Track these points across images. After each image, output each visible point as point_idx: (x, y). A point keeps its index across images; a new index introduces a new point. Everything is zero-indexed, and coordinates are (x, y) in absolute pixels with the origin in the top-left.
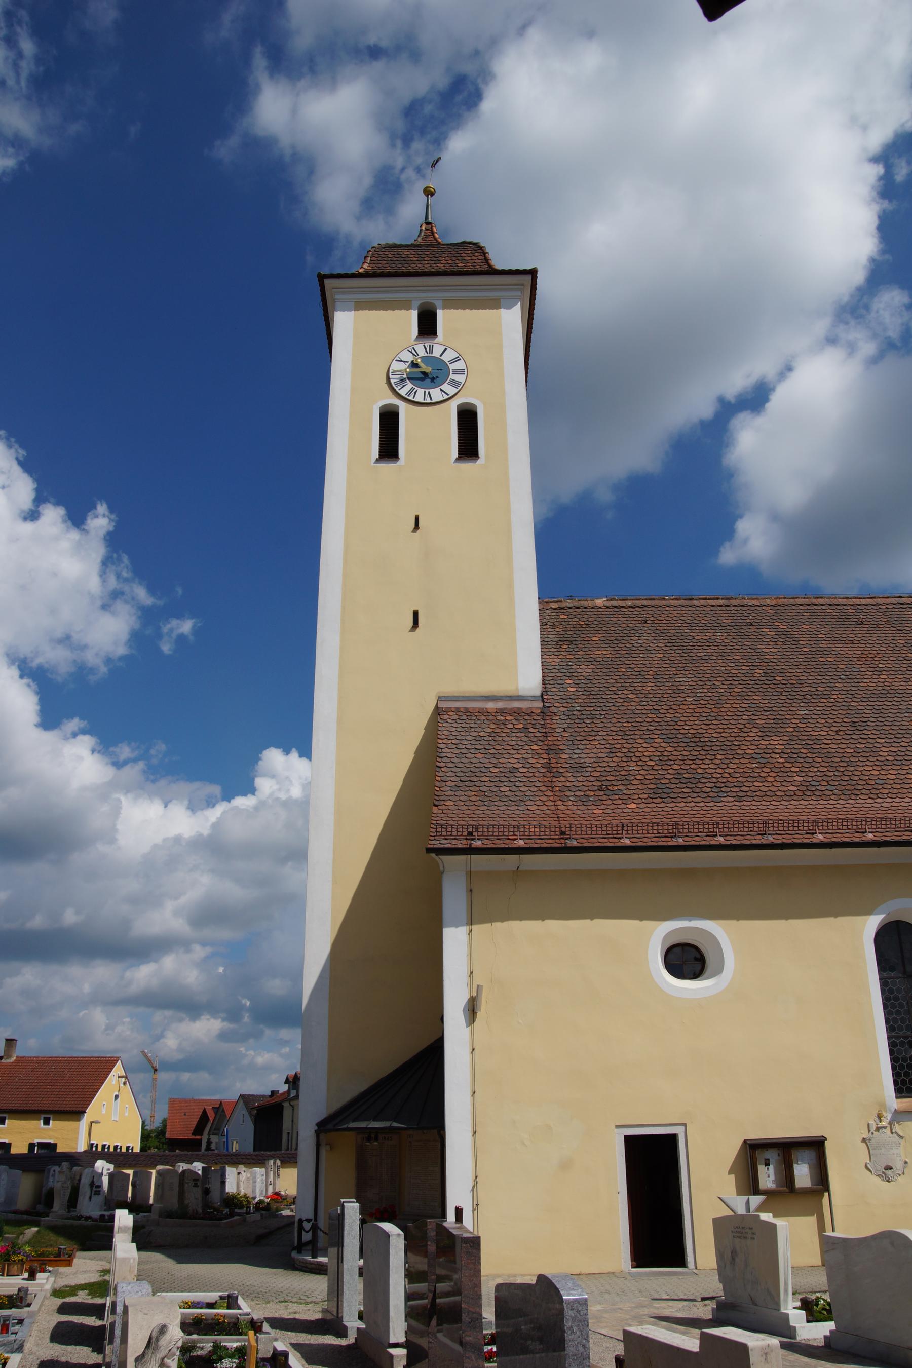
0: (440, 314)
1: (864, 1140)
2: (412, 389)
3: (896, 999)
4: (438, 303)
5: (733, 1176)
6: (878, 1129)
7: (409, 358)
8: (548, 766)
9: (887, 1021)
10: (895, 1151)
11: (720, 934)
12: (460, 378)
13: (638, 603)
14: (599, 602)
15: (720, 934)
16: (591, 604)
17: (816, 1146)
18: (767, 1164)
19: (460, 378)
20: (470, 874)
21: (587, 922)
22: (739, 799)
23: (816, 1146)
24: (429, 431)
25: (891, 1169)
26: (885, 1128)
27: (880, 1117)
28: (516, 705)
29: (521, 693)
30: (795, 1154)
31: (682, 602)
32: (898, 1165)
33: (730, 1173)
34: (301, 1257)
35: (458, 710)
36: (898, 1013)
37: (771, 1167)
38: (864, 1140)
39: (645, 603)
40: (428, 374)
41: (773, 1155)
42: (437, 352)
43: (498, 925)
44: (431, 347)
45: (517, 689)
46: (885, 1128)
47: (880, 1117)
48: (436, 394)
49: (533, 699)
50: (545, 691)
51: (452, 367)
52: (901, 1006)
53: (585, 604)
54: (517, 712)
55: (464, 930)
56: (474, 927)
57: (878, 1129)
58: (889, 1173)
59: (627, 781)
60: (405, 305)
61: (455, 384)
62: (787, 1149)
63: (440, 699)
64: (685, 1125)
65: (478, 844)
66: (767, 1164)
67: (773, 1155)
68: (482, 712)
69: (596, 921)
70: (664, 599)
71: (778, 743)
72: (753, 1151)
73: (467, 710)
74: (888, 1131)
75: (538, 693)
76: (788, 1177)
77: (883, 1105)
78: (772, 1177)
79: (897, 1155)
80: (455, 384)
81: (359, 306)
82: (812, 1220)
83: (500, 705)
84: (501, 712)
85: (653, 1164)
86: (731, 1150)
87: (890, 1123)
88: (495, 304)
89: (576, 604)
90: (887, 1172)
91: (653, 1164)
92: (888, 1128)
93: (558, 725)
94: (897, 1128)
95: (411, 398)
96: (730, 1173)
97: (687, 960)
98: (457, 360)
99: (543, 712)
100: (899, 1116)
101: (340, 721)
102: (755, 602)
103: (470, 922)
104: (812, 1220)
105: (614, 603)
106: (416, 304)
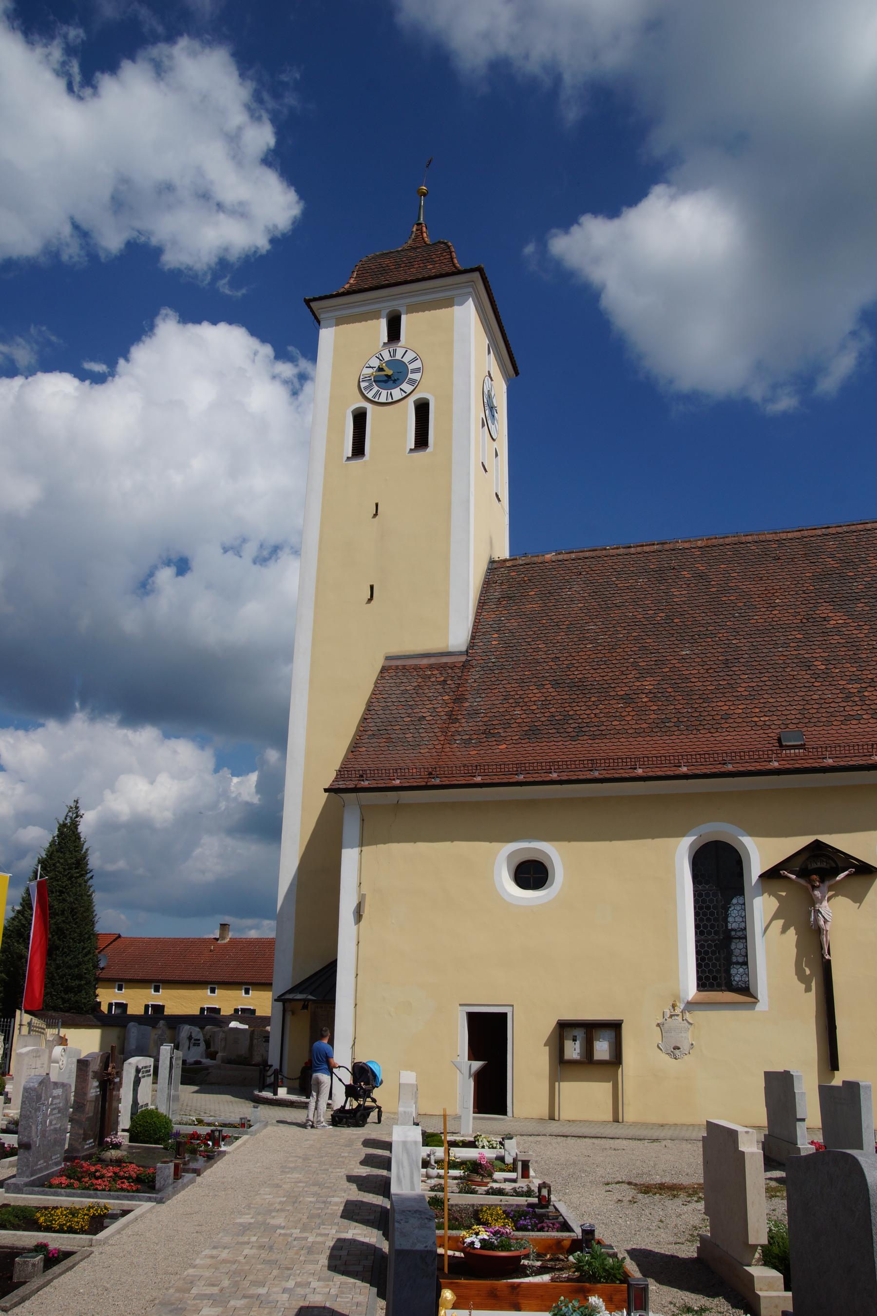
0: (404, 318)
1: (658, 1025)
2: (378, 391)
3: (708, 908)
4: (403, 309)
5: (547, 1048)
6: (671, 1016)
7: (376, 363)
8: (450, 715)
9: (697, 927)
10: (683, 1035)
11: (552, 851)
12: (416, 376)
13: (581, 555)
14: (548, 557)
15: (552, 851)
16: (540, 559)
17: (615, 1027)
18: (575, 1040)
19: (416, 376)
20: (361, 807)
21: (447, 844)
22: (594, 737)
23: (615, 1027)
24: (392, 426)
25: (679, 1048)
26: (677, 1015)
27: (674, 1006)
28: (445, 660)
29: (451, 649)
30: (596, 1033)
31: (621, 551)
32: (685, 1047)
33: (545, 1045)
34: (260, 1094)
35: (397, 667)
36: (708, 920)
37: (578, 1042)
38: (658, 1025)
39: (587, 554)
40: (390, 376)
41: (580, 1033)
42: (400, 353)
43: (381, 846)
44: (395, 351)
45: (448, 646)
46: (677, 1015)
47: (674, 1006)
48: (397, 394)
49: (460, 653)
50: (472, 645)
51: (411, 367)
52: (712, 914)
53: (535, 559)
54: (442, 667)
55: (357, 850)
56: (363, 848)
57: (671, 1016)
58: (677, 1052)
59: (507, 725)
60: (375, 315)
61: (412, 382)
62: (590, 1029)
63: (387, 658)
64: (512, 1006)
65: (365, 784)
66: (575, 1040)
67: (580, 1033)
68: (416, 668)
69: (456, 843)
70: (605, 549)
71: (648, 684)
72: (564, 1028)
73: (404, 667)
74: (679, 1018)
75: (464, 648)
76: (589, 1049)
77: (677, 997)
78: (578, 1051)
79: (686, 1039)
80: (412, 382)
81: (340, 321)
82: (608, 1086)
83: (433, 661)
84: (431, 667)
85: (488, 1034)
86: (549, 1026)
87: (682, 1012)
88: (449, 303)
89: (528, 561)
90: (675, 1051)
91: (488, 1034)
92: (681, 1016)
93: (474, 675)
94: (687, 1015)
95: (376, 400)
96: (545, 1045)
97: (532, 874)
99: (465, 666)
100: (691, 1006)
101: (311, 682)
102: (686, 545)
103: (362, 844)
104: (608, 1086)
105: (560, 557)
106: (385, 313)
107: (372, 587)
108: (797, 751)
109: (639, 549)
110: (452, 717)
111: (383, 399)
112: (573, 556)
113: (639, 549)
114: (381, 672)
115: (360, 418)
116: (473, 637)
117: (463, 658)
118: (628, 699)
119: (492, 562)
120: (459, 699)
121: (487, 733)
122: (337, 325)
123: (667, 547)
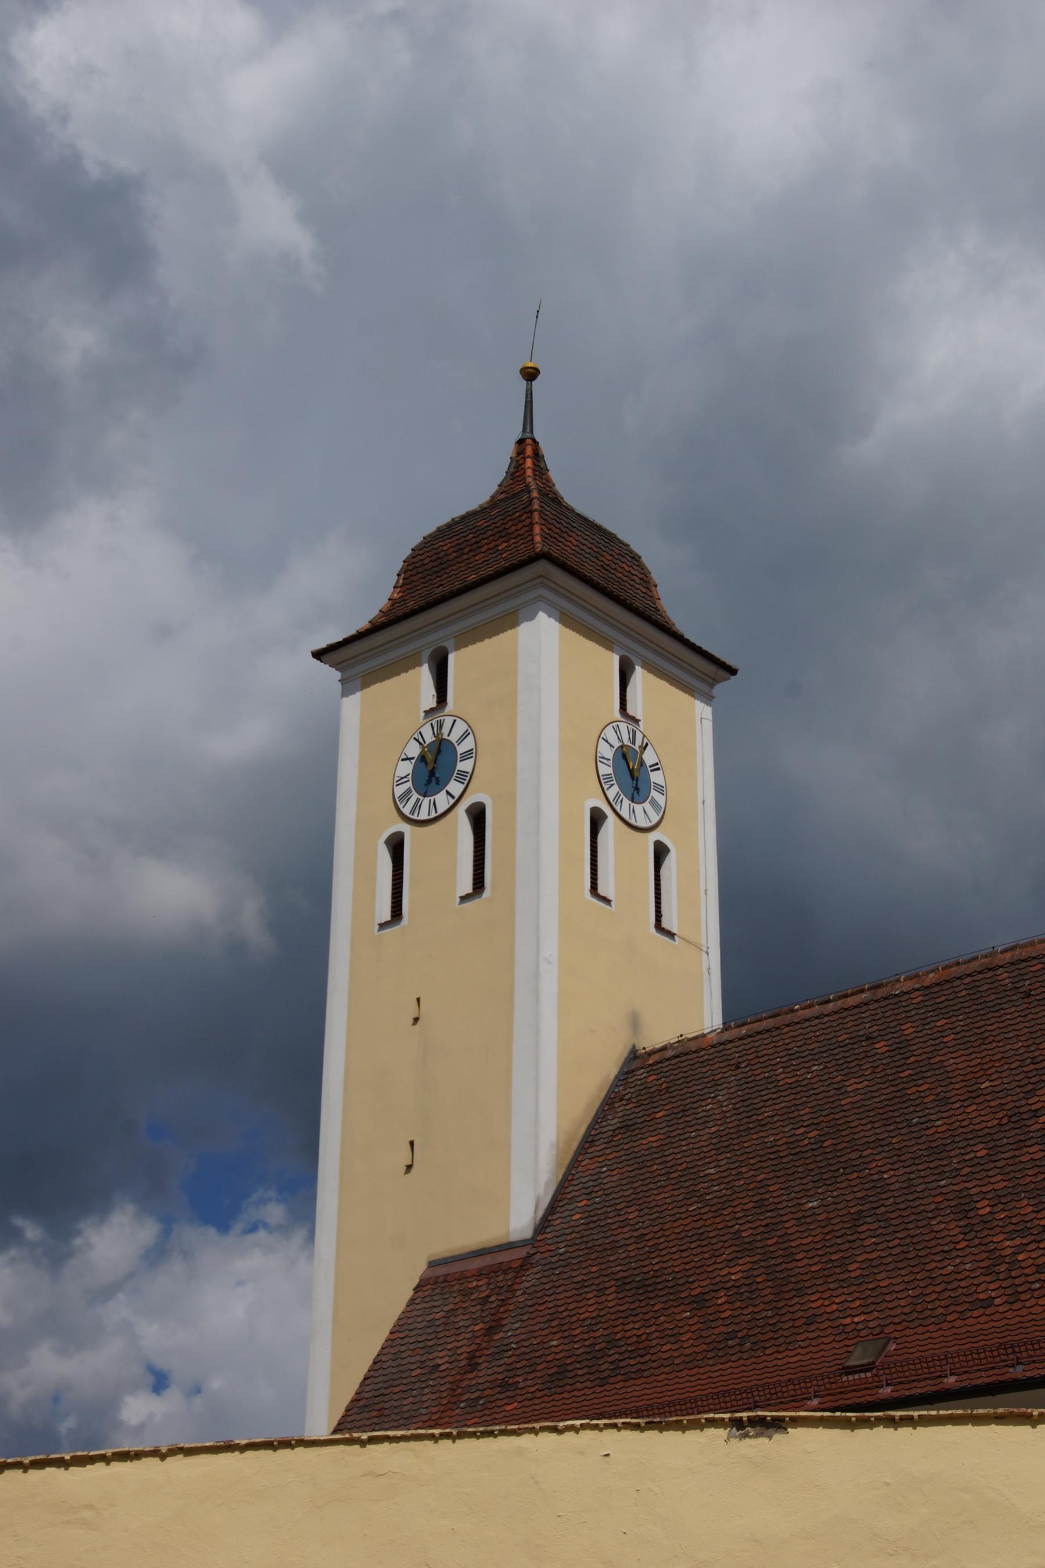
0: (452, 658)
2: (418, 800)
4: (449, 644)
7: (414, 750)
8: (472, 1356)
24: (443, 853)
40: (434, 766)
44: (440, 725)
45: (508, 1233)
48: (442, 801)
50: (543, 1225)
51: (461, 749)
60: (410, 663)
68: (462, 1277)
70: (792, 1011)
75: (528, 1234)
83: (487, 1261)
84: (479, 1274)
88: (510, 621)
93: (530, 1279)
95: (415, 817)
98: (465, 735)
99: (525, 1264)
106: (426, 654)
107: (412, 1143)
108: (863, 1375)
109: (840, 1004)
110: (473, 1365)
111: (423, 815)
112: (744, 1031)
113: (840, 1004)
114: (416, 1290)
115: (396, 846)
116: (552, 1208)
117: (522, 1253)
118: (700, 1302)
119: (634, 1055)
120: (490, 1331)
121: (505, 1385)
122: (365, 685)
123: (881, 993)
